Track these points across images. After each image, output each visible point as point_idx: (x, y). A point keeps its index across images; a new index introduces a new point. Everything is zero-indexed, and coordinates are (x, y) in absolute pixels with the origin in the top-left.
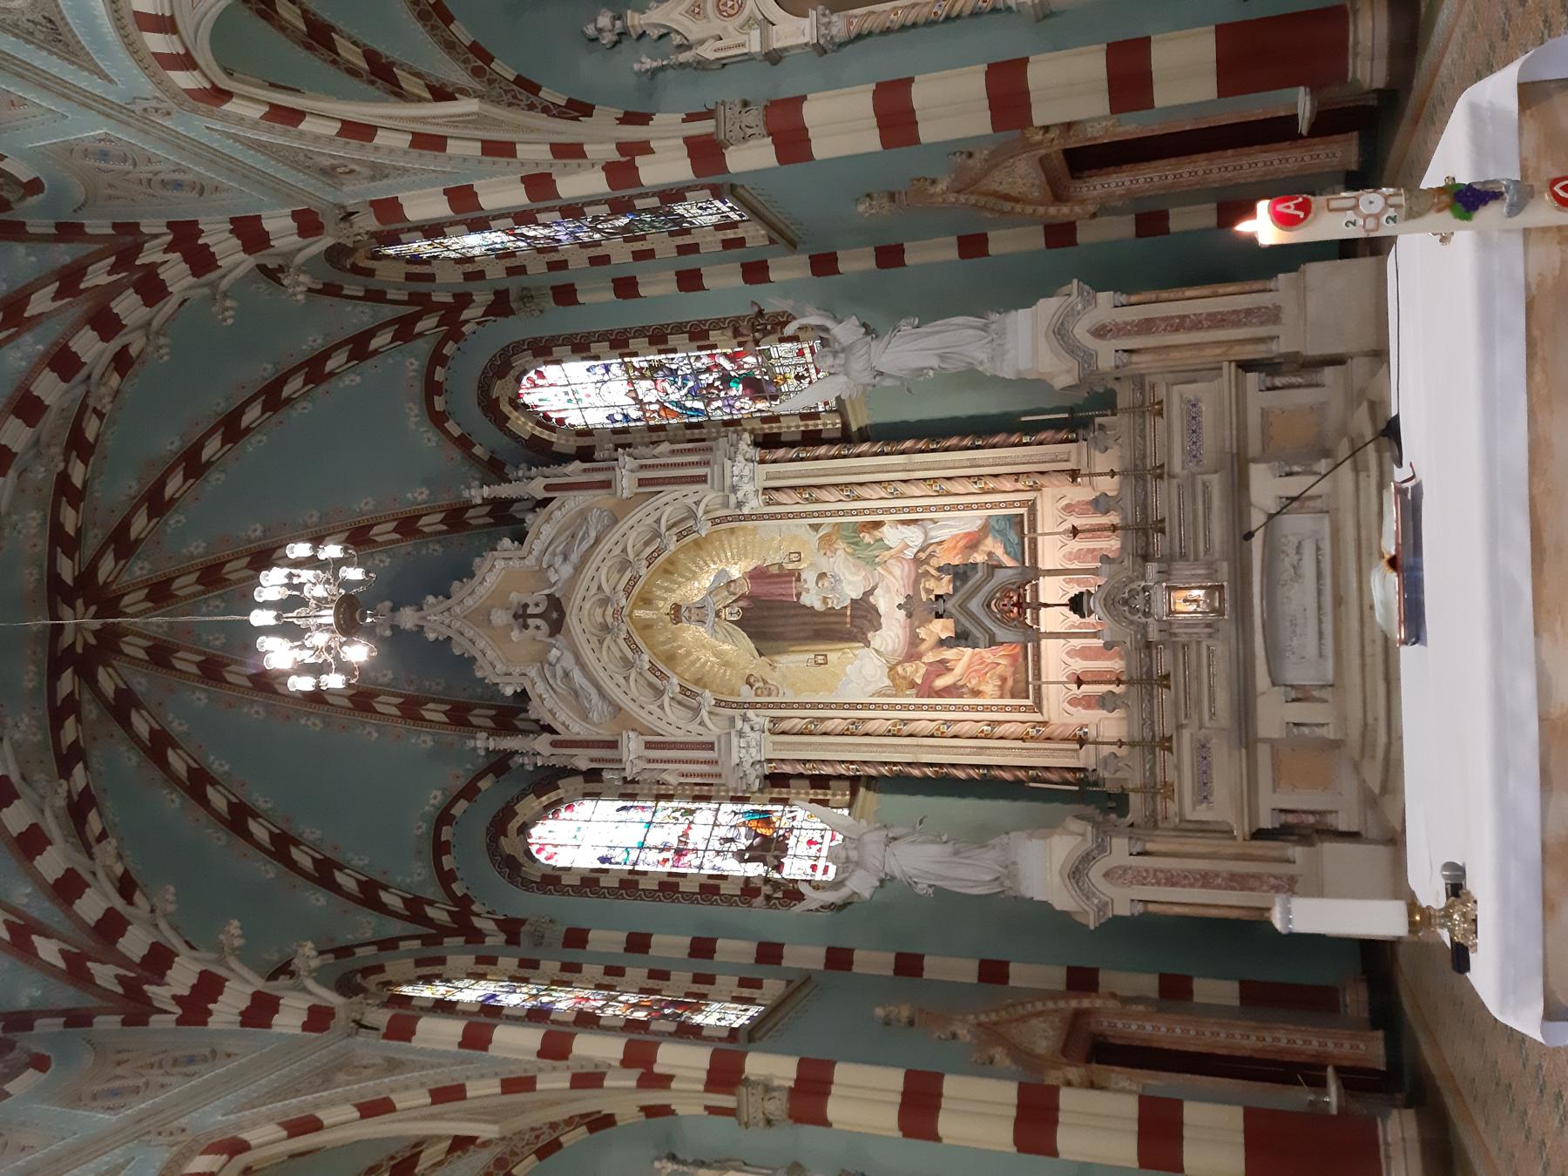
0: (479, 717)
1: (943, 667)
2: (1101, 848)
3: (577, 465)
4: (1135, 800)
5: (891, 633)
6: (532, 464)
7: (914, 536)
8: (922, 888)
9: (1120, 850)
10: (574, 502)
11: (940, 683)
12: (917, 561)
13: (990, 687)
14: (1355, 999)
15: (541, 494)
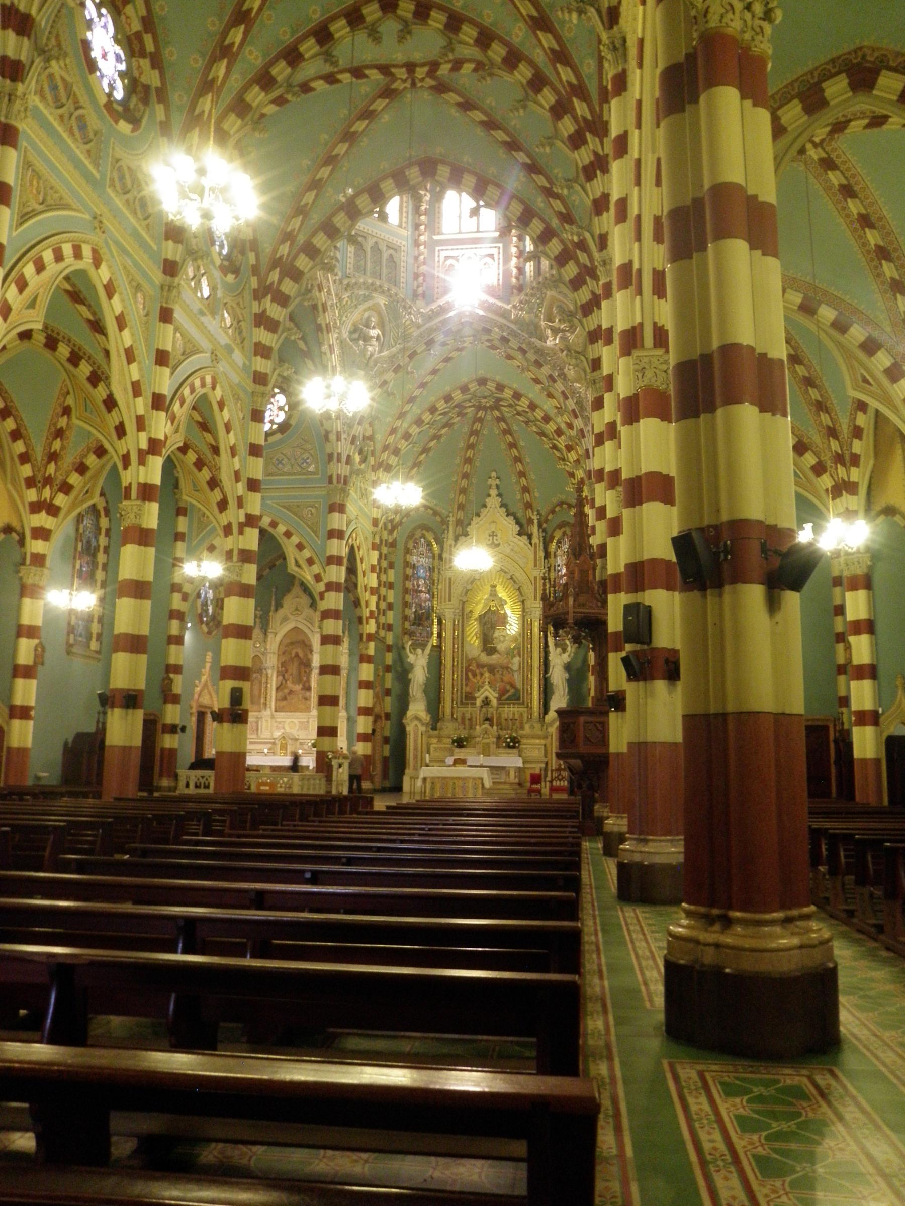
0: (460, 514)
1: (475, 675)
2: (423, 724)
3: (542, 554)
4: (436, 732)
5: (484, 658)
6: (544, 538)
7: (515, 667)
8: (410, 676)
9: (422, 728)
10: (531, 556)
11: (470, 675)
12: (507, 668)
13: (468, 689)
14: (387, 784)
15: (533, 542)
